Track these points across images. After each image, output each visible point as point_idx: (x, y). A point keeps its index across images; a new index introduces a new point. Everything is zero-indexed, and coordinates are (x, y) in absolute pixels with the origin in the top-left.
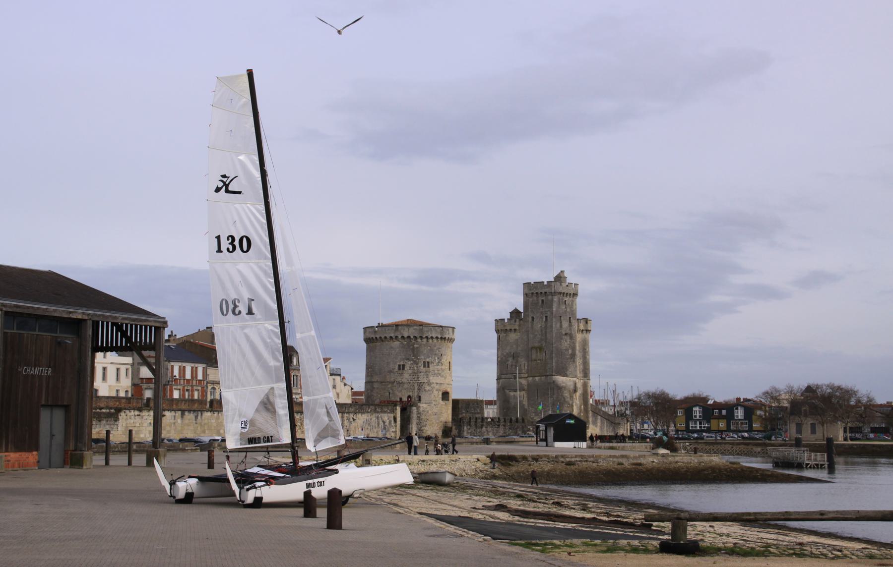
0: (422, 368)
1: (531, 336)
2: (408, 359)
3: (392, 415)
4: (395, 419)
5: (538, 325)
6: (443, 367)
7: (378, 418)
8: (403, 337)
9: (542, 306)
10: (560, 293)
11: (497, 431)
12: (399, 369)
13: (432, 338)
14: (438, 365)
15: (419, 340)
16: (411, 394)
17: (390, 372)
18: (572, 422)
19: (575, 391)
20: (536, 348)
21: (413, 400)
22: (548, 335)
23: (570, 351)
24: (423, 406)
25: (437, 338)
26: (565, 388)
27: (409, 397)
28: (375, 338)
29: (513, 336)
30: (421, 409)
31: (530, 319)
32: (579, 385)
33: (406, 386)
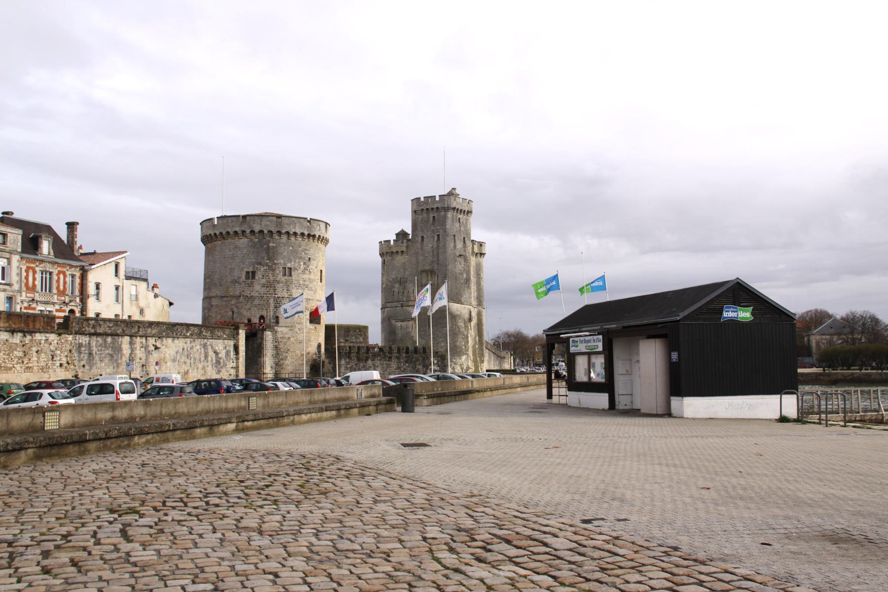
0: (280, 277)
1: (421, 258)
2: (260, 264)
3: (232, 343)
4: (236, 348)
5: (429, 245)
6: (312, 277)
7: (205, 346)
8: (252, 232)
9: (433, 224)
10: (454, 209)
11: (389, 366)
12: (247, 278)
13: (295, 234)
14: (303, 272)
15: (276, 237)
16: (264, 313)
17: (235, 282)
18: (745, 314)
19: (470, 320)
20: (426, 271)
21: (267, 322)
22: (441, 257)
23: (465, 275)
24: (281, 330)
25: (303, 234)
26: (459, 316)
27: (262, 317)
28: (217, 235)
29: (399, 260)
30: (279, 335)
31: (420, 239)
32: (474, 314)
33: (256, 302)
